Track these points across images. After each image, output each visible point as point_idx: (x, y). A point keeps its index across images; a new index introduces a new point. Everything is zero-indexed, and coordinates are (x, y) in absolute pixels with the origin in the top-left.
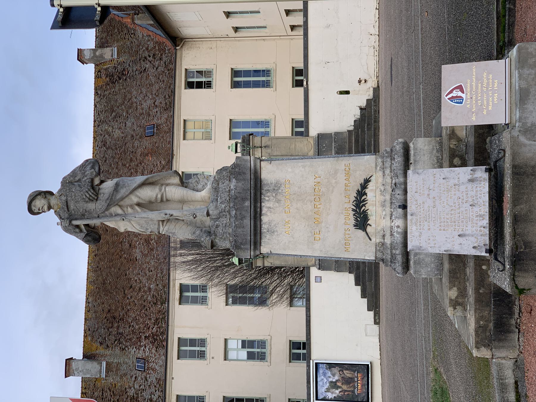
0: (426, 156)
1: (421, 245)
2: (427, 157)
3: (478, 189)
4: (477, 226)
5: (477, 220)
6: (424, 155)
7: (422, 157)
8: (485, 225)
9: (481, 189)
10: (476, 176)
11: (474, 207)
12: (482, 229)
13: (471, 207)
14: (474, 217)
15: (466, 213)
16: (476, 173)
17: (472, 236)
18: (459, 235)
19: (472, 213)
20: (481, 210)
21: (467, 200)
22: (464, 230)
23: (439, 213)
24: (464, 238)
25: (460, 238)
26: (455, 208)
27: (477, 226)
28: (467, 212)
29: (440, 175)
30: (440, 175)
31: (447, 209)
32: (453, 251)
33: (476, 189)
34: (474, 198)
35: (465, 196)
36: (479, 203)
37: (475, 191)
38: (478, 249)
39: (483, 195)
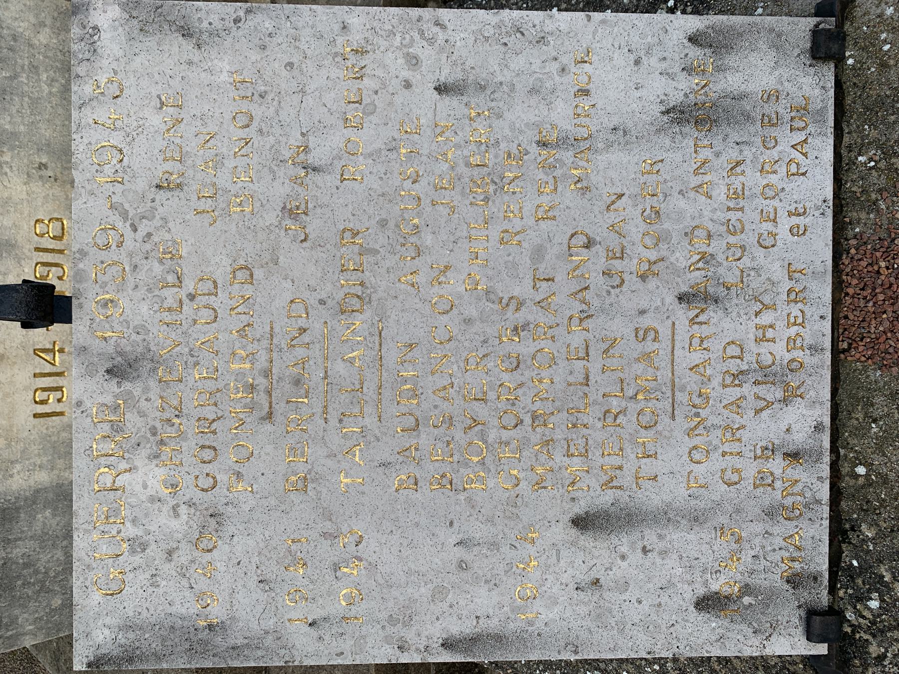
0: (44, 77)
1: (217, 612)
2: (50, 85)
3: (752, 179)
4: (735, 447)
5: (737, 405)
6: (34, 69)
7: (23, 78)
8: (800, 437)
9: (773, 179)
10: (732, 82)
11: (713, 314)
12: (777, 465)
13: (683, 315)
14: (716, 382)
15: (647, 357)
16: (731, 60)
17: (696, 519)
18: (581, 523)
19: (697, 357)
20: (770, 334)
21: (653, 255)
22: (627, 479)
23: (392, 355)
24: (624, 542)
25: (586, 540)
26: (543, 319)
27: (735, 447)
28: (650, 346)
29: (414, 62)
30: (414, 62)
31: (468, 321)
32: (521, 639)
33: (737, 182)
34: (717, 247)
35: (635, 229)
36: (756, 283)
37: (720, 193)
38: (744, 615)
39: (785, 223)
